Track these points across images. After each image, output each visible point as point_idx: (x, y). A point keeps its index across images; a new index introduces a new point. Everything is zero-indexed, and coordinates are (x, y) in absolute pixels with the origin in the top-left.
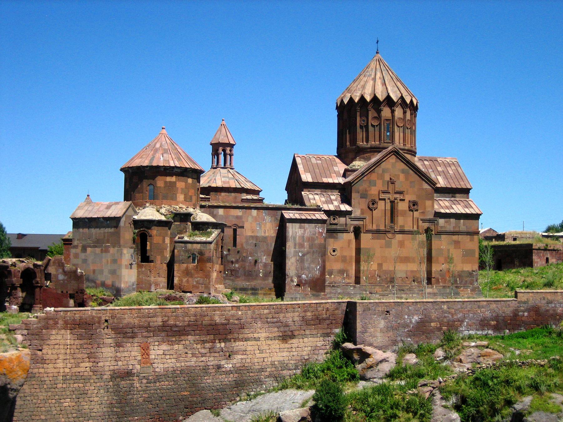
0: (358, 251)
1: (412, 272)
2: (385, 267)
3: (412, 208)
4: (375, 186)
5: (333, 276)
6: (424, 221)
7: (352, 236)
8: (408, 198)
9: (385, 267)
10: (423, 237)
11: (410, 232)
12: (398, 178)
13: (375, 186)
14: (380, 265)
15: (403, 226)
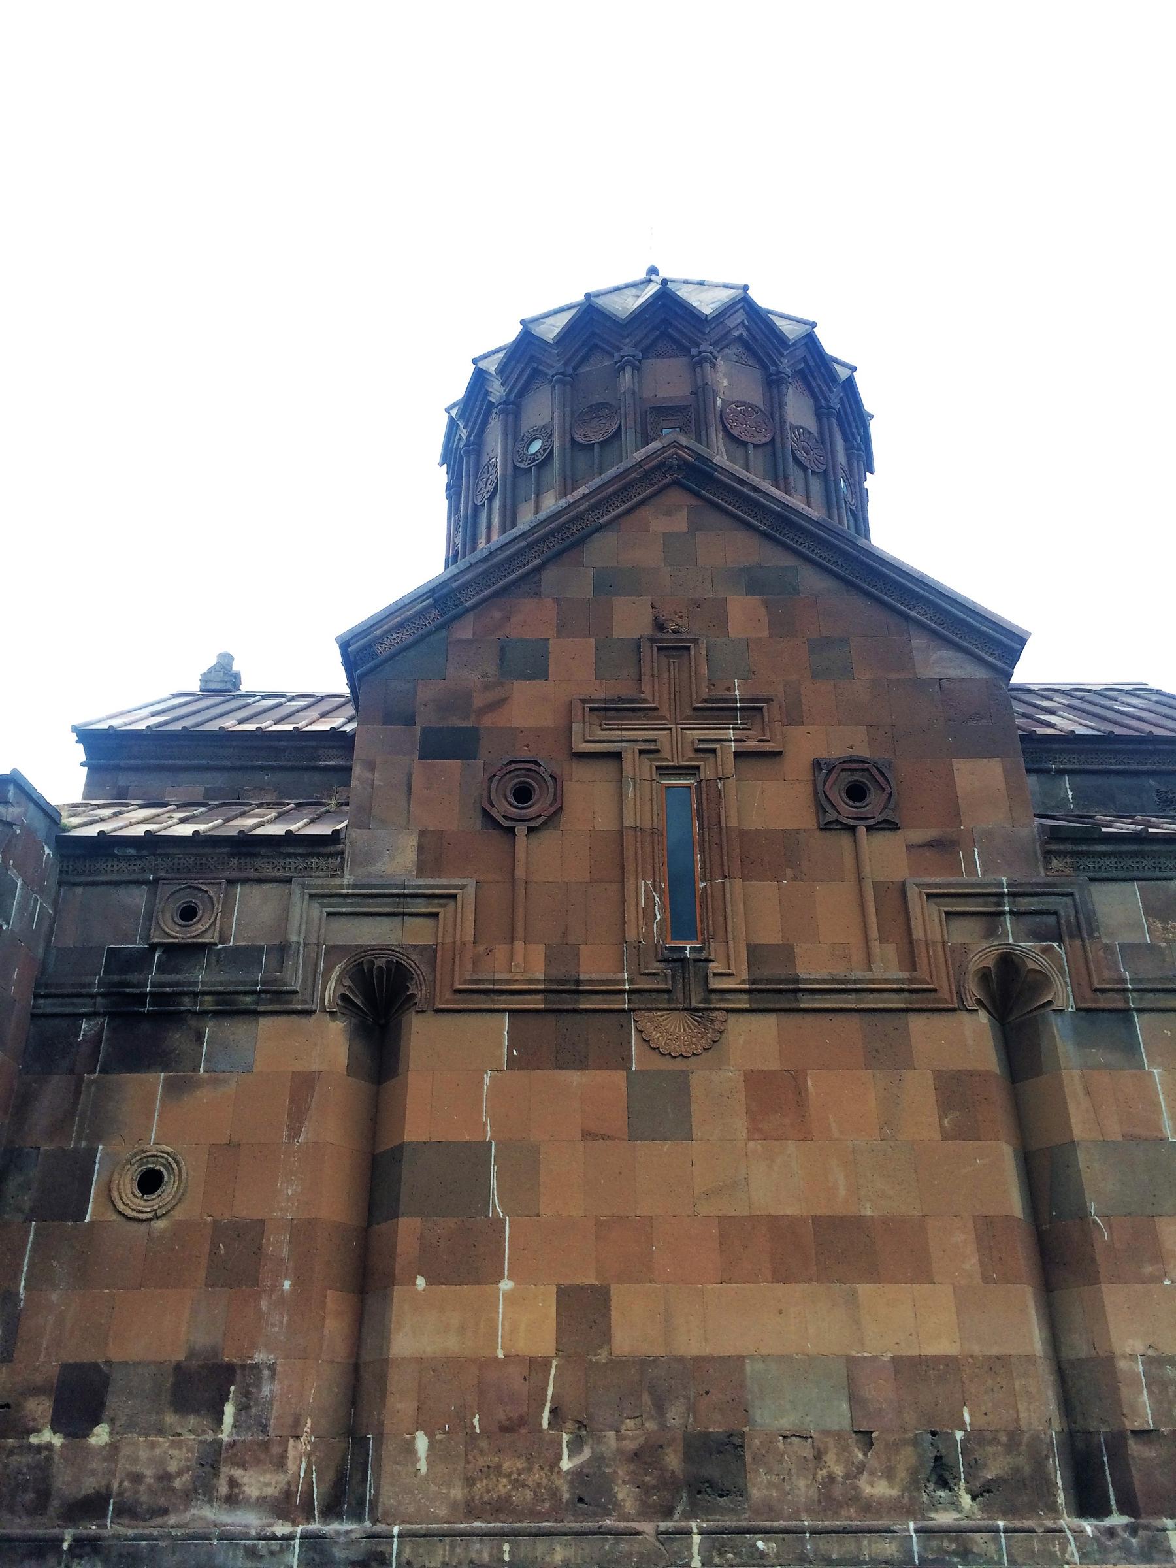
0: (380, 1175)
1: (911, 1369)
2: (633, 1330)
3: (847, 809)
4: (540, 672)
5: (101, 1435)
6: (956, 903)
7: (329, 1044)
8: (808, 744)
9: (633, 1330)
10: (971, 1039)
11: (842, 998)
12: (721, 622)
13: (543, 674)
14: (583, 1310)
15: (786, 952)
